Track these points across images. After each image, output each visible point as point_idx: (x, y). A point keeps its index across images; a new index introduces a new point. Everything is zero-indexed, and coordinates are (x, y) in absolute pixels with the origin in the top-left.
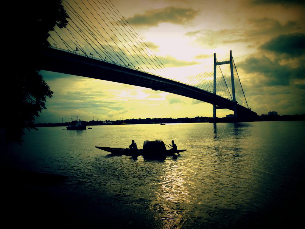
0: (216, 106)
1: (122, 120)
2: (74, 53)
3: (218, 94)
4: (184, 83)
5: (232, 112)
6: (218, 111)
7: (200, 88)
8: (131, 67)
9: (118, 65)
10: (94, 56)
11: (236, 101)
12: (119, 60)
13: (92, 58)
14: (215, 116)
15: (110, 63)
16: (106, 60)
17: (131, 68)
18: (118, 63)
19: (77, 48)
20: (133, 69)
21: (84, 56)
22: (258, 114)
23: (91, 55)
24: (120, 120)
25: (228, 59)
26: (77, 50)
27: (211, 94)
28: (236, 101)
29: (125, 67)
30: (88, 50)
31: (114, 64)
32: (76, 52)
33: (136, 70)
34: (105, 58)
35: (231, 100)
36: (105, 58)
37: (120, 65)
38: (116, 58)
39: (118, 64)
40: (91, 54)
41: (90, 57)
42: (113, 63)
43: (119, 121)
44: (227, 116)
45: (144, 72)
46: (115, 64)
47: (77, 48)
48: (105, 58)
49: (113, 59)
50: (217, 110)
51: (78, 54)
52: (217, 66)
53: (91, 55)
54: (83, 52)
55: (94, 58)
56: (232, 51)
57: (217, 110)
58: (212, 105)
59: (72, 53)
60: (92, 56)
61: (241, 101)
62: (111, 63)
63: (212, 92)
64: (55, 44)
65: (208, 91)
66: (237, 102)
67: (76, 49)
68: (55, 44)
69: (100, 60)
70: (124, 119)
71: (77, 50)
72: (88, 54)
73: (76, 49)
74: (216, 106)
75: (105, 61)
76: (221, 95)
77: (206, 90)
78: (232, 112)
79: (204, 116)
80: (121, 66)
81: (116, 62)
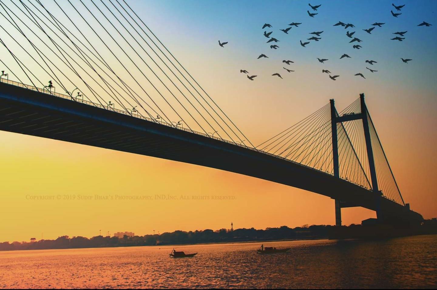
3: (342, 175)
6: (344, 211)
8: (163, 121)
9: (136, 117)
10: (85, 99)
11: (379, 190)
12: (138, 108)
16: (110, 106)
17: (163, 124)
18: (136, 113)
19: (50, 82)
20: (168, 125)
25: (358, 111)
26: (51, 86)
28: (379, 190)
29: (150, 120)
32: (49, 90)
34: (110, 102)
35: (369, 189)
36: (109, 103)
37: (139, 117)
38: (135, 104)
39: (135, 115)
41: (77, 101)
45: (190, 131)
47: (50, 82)
48: (110, 102)
52: (338, 125)
59: (40, 91)
60: (81, 98)
63: (330, 171)
64: (5, 73)
65: (322, 171)
67: (49, 84)
68: (5, 73)
71: (51, 86)
72: (75, 95)
73: (49, 84)
75: (109, 109)
76: (348, 178)
80: (142, 118)
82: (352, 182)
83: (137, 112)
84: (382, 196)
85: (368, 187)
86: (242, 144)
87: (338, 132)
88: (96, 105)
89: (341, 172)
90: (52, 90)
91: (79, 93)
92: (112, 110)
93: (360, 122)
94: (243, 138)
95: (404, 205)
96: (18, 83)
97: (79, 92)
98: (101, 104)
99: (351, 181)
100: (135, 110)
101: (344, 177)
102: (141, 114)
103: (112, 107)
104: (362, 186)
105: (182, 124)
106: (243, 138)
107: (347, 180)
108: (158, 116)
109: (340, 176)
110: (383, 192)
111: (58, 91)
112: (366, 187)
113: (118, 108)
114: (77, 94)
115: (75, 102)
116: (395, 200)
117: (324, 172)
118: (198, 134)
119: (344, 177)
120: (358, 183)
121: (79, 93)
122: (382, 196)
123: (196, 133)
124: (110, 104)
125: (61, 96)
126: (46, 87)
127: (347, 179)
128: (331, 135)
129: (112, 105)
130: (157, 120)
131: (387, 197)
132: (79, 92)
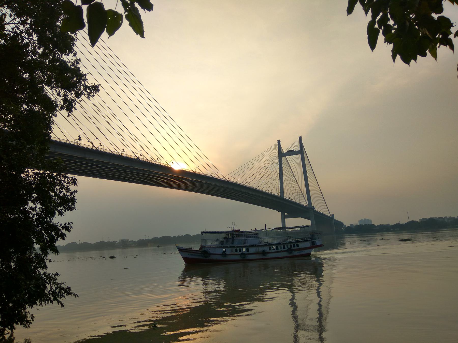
0: (286, 214)
2: (76, 144)
4: (239, 182)
5: (307, 222)
7: (261, 189)
8: (162, 162)
10: (105, 148)
12: (143, 152)
13: (102, 150)
15: (130, 157)
17: (161, 164)
19: (79, 136)
20: (165, 165)
21: (91, 147)
26: (80, 139)
29: (152, 162)
30: (97, 139)
31: (136, 158)
32: (79, 142)
33: (168, 165)
34: (123, 150)
35: (305, 205)
36: (122, 151)
39: (141, 158)
41: (99, 149)
42: (134, 158)
46: (138, 158)
47: (79, 136)
48: (123, 150)
49: (134, 150)
51: (81, 145)
54: (88, 141)
55: (105, 151)
56: (302, 137)
59: (72, 143)
61: (319, 207)
62: (132, 157)
63: (278, 194)
66: (314, 208)
67: (78, 138)
69: (115, 153)
71: (80, 139)
73: (78, 138)
74: (286, 214)
75: (123, 155)
76: (291, 198)
77: (270, 192)
78: (307, 222)
80: (147, 161)
81: (138, 155)
82: (293, 201)
84: (315, 210)
85: (305, 203)
86: (216, 176)
88: (113, 152)
89: (285, 193)
90: (81, 142)
91: (100, 144)
92: (125, 156)
95: (331, 216)
97: (101, 143)
100: (141, 155)
101: (288, 197)
102: (145, 157)
104: (301, 203)
107: (290, 199)
108: (157, 159)
109: (284, 196)
111: (85, 143)
112: (303, 204)
113: (129, 154)
114: (100, 145)
115: (98, 150)
118: (188, 171)
119: (288, 197)
120: (298, 201)
121: (100, 144)
122: (315, 210)
124: (123, 151)
125: (88, 147)
126: (76, 140)
127: (290, 199)
130: (157, 161)
131: (320, 211)
132: (101, 143)
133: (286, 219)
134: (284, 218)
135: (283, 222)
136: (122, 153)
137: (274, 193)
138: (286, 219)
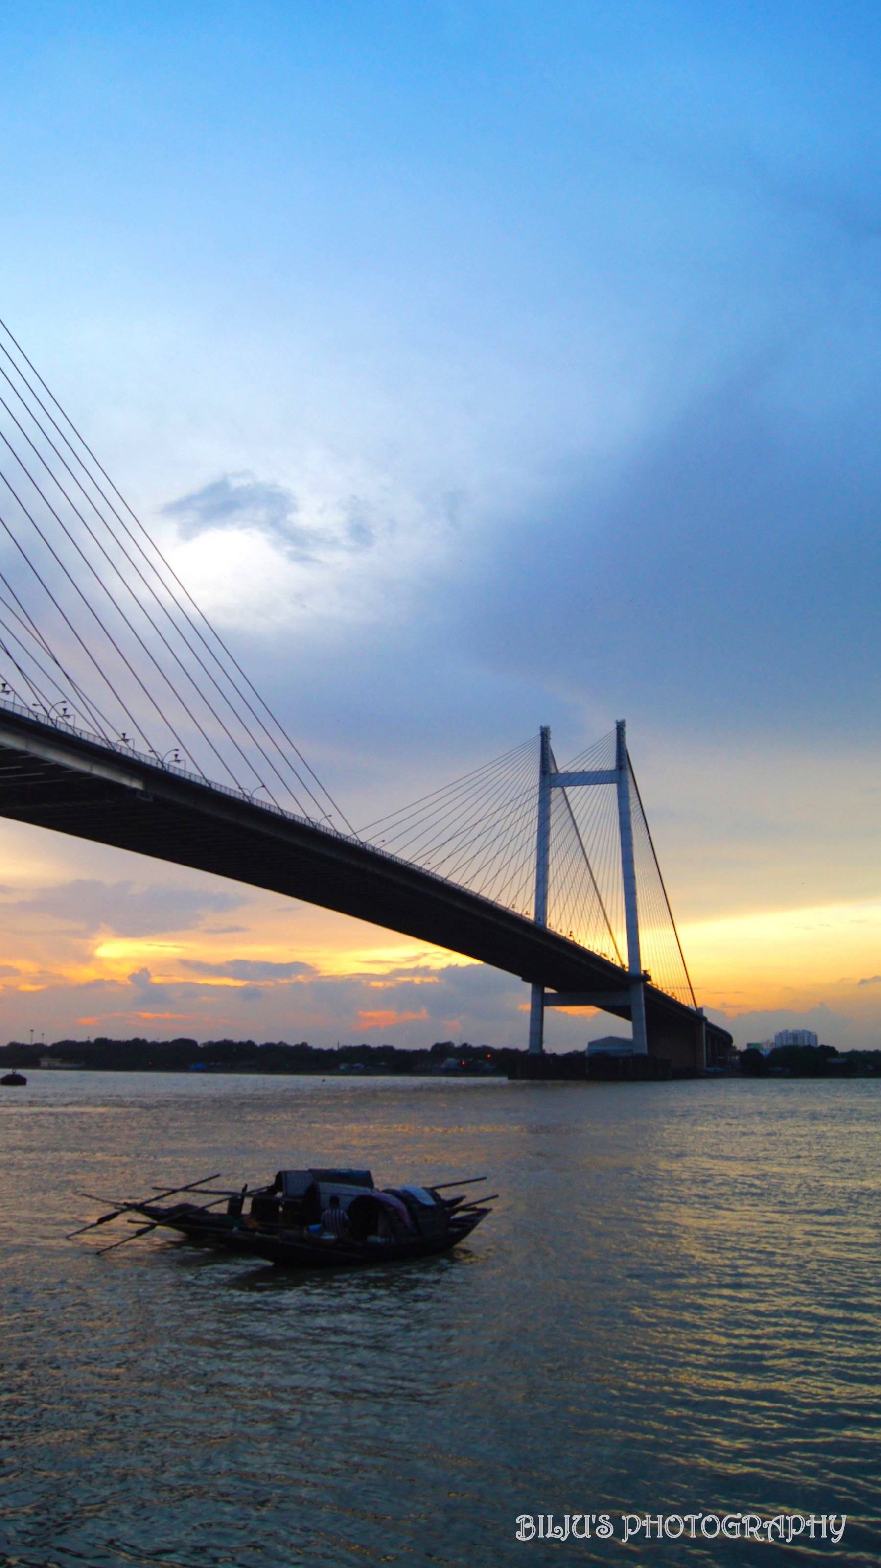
0: (548, 990)
1: (37, 1040)
11: (643, 968)
14: (541, 1042)
22: (734, 1044)
23: (8, 692)
24: (25, 1039)
27: (517, 921)
36: (62, 713)
40: (8, 688)
43: (23, 1047)
44: (590, 1044)
50: (548, 1010)
53: (8, 692)
57: (548, 1010)
58: (529, 986)
63: (528, 911)
65: (516, 910)
70: (49, 1042)
75: (63, 728)
76: (574, 934)
79: (475, 1043)
83: (12, 693)
84: (649, 983)
87: (553, 806)
91: (4, 685)
93: (612, 789)
94: (329, 809)
96: (5, 701)
98: (24, 703)
99: (580, 941)
103: (70, 721)
105: (184, 761)
106: (329, 809)
110: (652, 973)
116: (677, 996)
117: (520, 912)
122: (649, 983)
123: (218, 789)
127: (570, 935)
128: (535, 812)
129: (68, 716)
131: (660, 986)
133: (546, 1009)
134: (540, 1002)
135: (537, 1020)
136: (60, 719)
137: (519, 910)
138: (546, 1009)
